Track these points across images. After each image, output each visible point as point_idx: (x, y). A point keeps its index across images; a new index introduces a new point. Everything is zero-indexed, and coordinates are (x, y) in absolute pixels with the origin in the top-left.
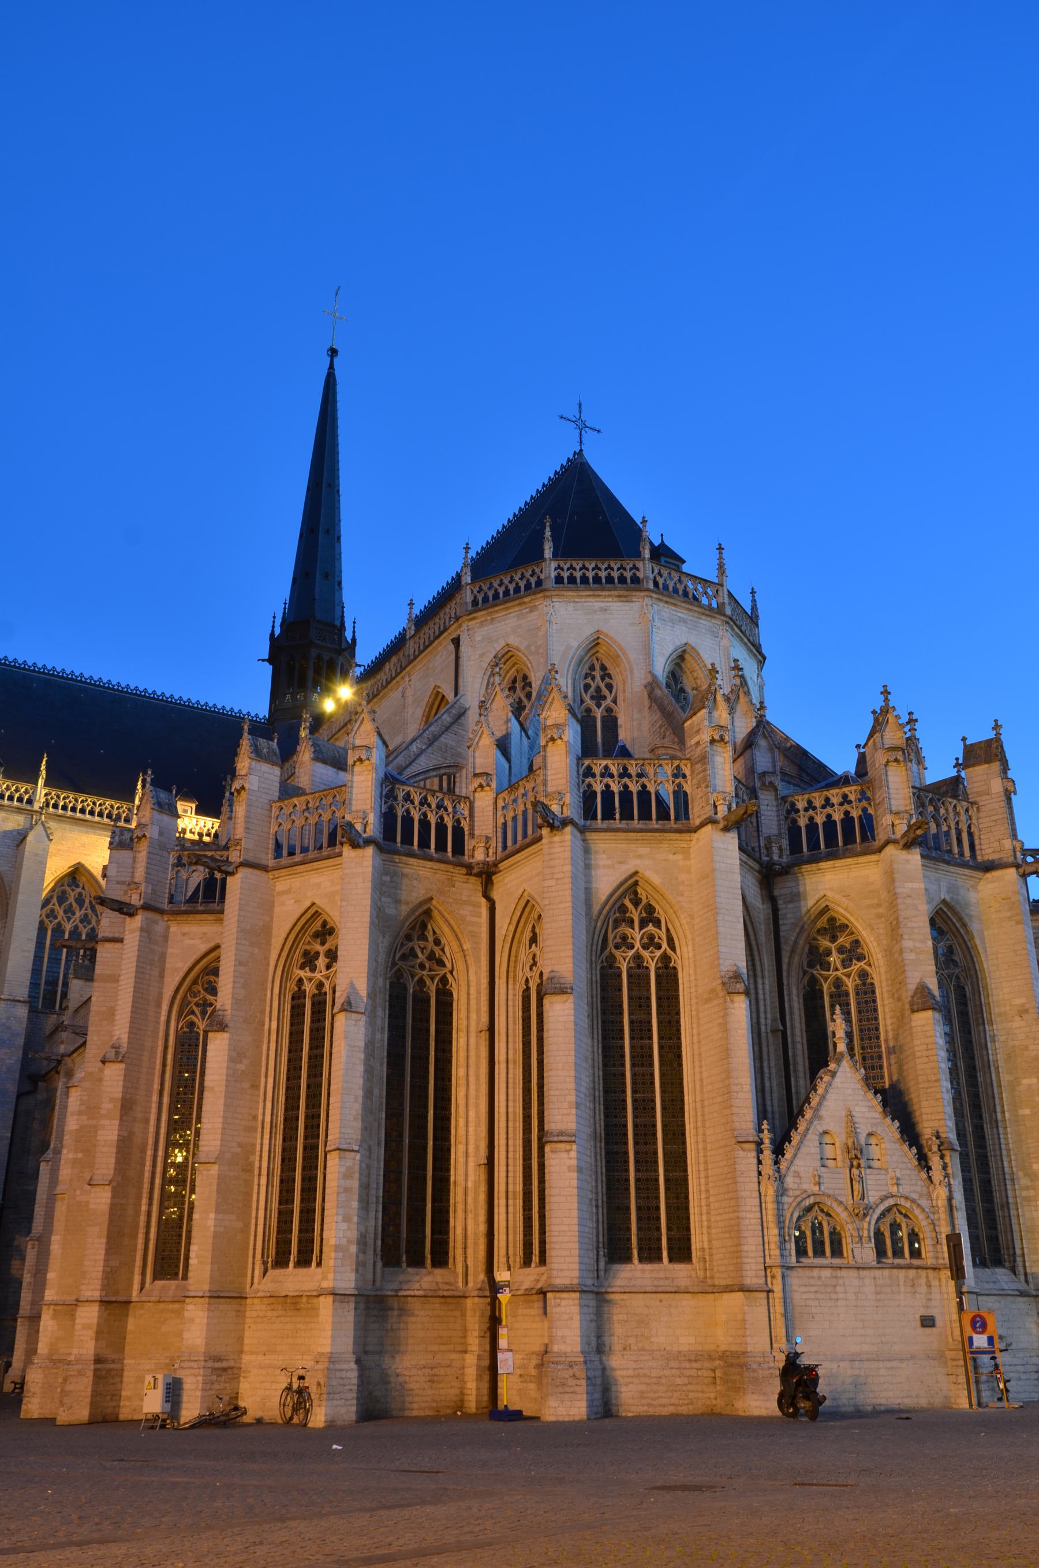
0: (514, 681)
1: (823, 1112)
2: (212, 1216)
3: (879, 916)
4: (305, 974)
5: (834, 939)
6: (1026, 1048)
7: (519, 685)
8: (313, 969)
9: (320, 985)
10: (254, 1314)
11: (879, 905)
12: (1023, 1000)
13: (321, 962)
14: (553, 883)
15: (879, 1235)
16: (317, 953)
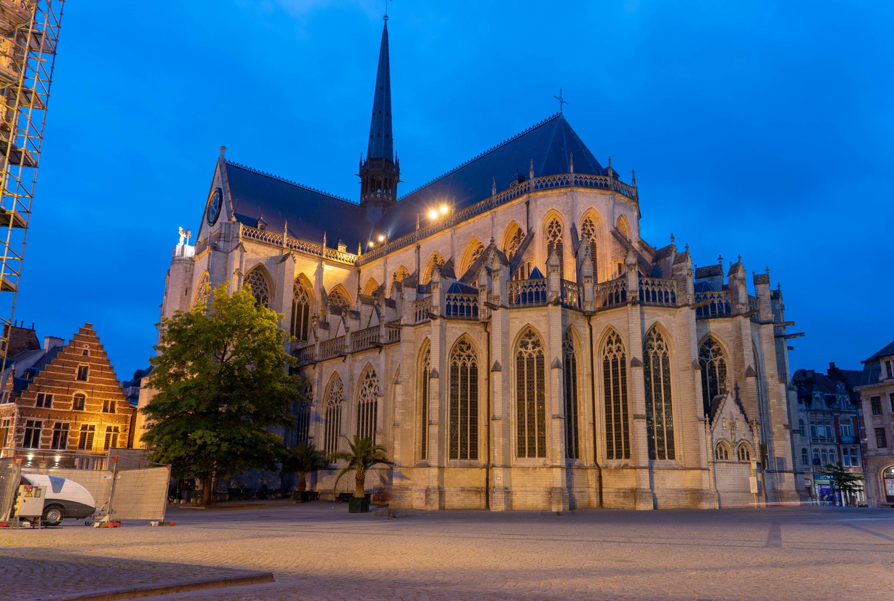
0: (552, 223)
1: (723, 411)
2: (501, 439)
3: (731, 340)
4: (523, 350)
5: (710, 347)
6: (773, 389)
7: (555, 225)
8: (527, 348)
9: (530, 355)
10: (515, 473)
11: (731, 337)
12: (773, 372)
13: (530, 346)
14: (633, 325)
15: (738, 452)
16: (528, 343)
